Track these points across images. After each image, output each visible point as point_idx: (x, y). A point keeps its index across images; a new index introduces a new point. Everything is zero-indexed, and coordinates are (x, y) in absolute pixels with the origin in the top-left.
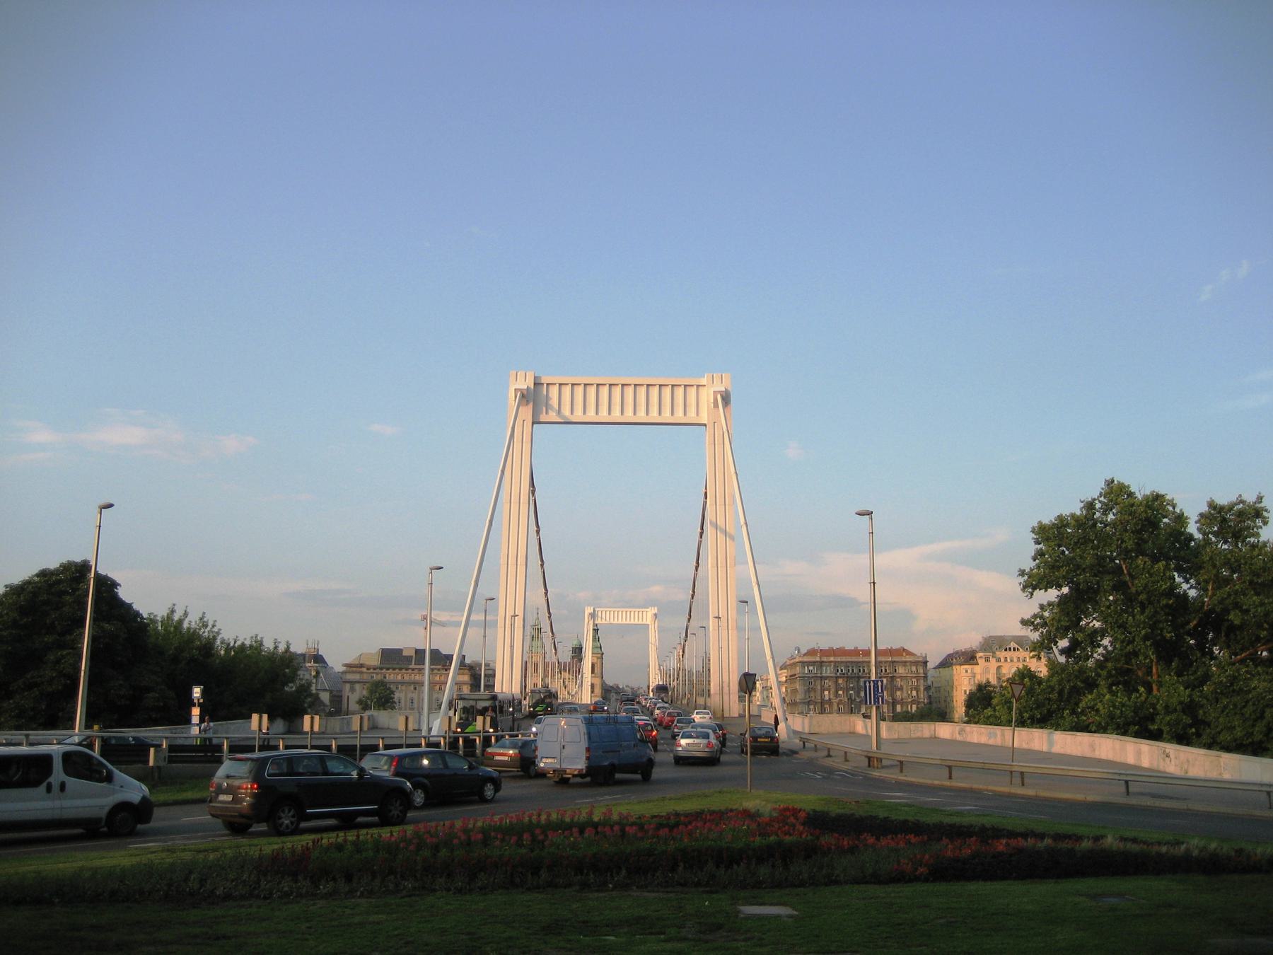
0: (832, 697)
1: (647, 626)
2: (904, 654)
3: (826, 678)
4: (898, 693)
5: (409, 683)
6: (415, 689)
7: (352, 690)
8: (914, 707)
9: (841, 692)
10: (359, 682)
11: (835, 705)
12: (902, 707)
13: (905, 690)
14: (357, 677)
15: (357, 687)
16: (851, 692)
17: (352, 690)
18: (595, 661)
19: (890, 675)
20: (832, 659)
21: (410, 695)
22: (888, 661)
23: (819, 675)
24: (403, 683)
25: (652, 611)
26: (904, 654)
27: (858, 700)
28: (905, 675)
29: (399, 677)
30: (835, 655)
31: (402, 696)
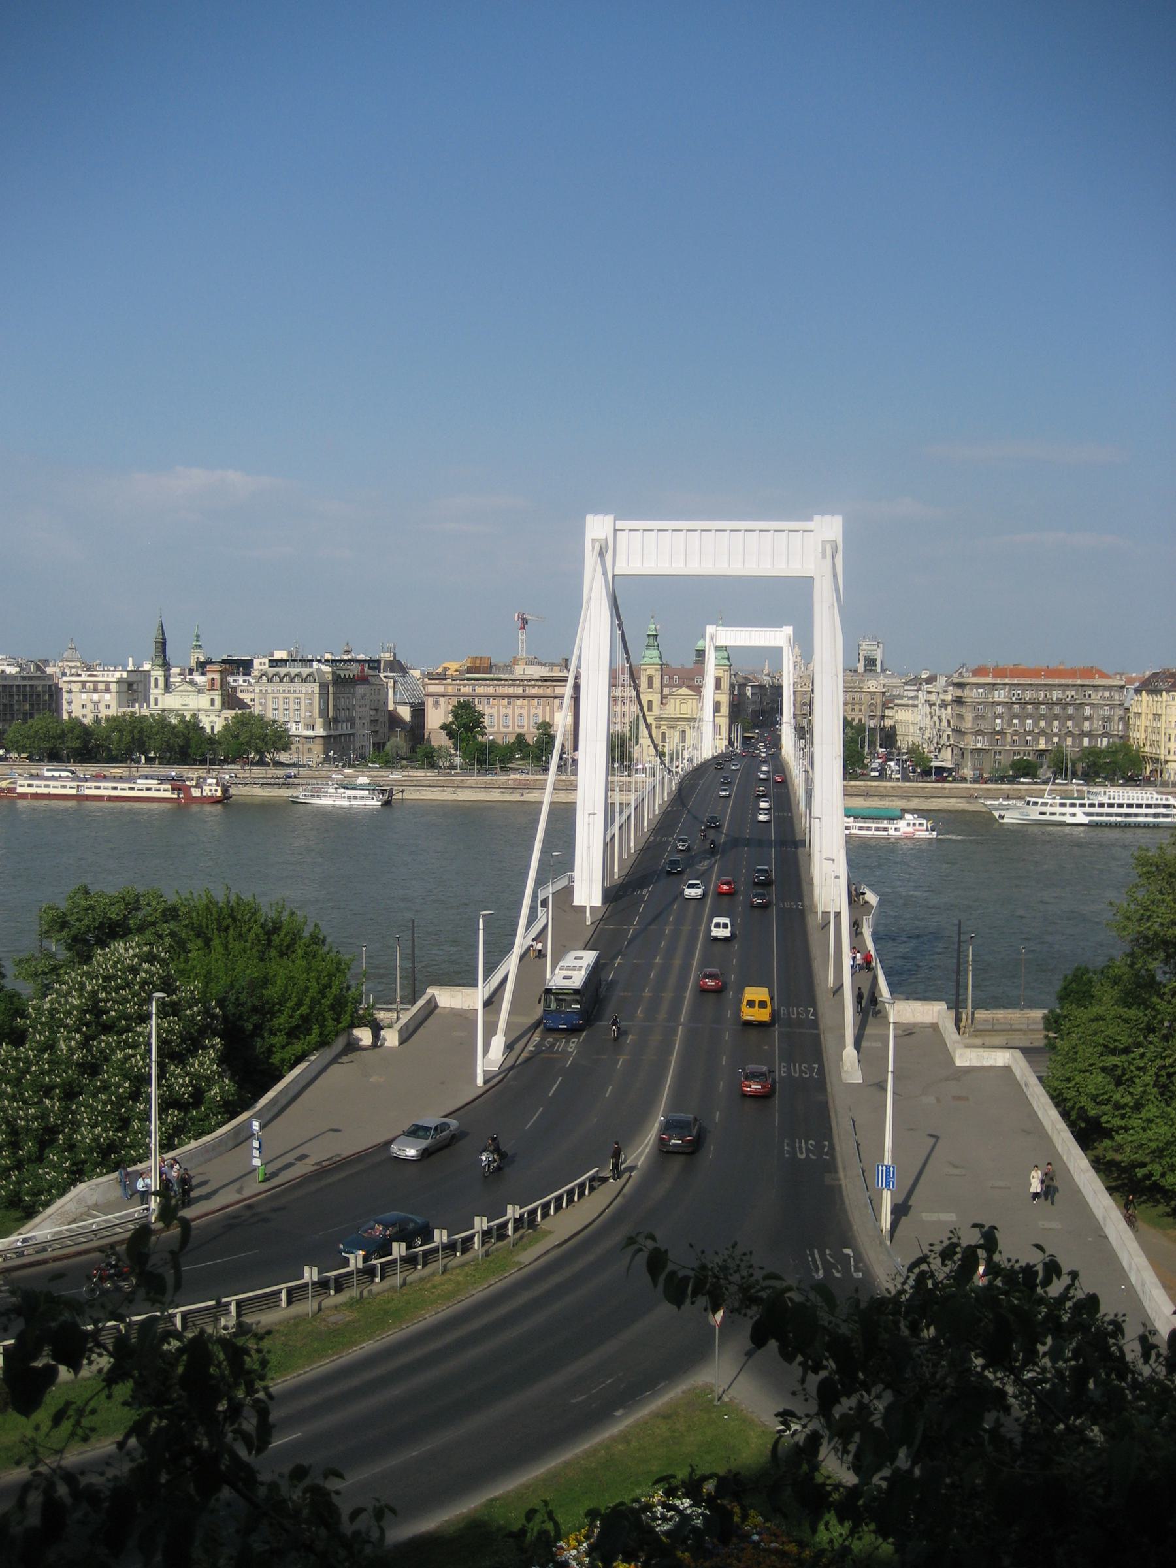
0: (1005, 727)
1: (779, 650)
2: (1097, 676)
3: (999, 703)
4: (1087, 724)
5: (503, 697)
6: (509, 703)
7: (436, 704)
8: (1105, 741)
9: (1015, 721)
10: (444, 696)
11: (1009, 736)
12: (1090, 741)
13: (1095, 722)
14: (439, 689)
15: (442, 700)
16: (1029, 721)
17: (436, 704)
18: (721, 673)
19: (1078, 702)
20: (1007, 681)
21: (503, 711)
22: (1075, 685)
23: (990, 700)
24: (494, 697)
25: (788, 630)
26: (1097, 676)
27: (1037, 731)
28: (1096, 702)
29: (491, 690)
30: (1012, 677)
31: (494, 711)
